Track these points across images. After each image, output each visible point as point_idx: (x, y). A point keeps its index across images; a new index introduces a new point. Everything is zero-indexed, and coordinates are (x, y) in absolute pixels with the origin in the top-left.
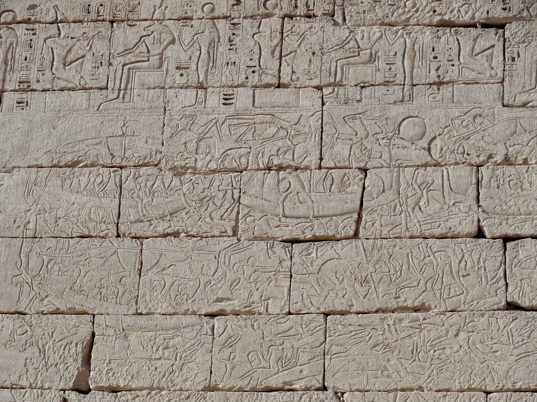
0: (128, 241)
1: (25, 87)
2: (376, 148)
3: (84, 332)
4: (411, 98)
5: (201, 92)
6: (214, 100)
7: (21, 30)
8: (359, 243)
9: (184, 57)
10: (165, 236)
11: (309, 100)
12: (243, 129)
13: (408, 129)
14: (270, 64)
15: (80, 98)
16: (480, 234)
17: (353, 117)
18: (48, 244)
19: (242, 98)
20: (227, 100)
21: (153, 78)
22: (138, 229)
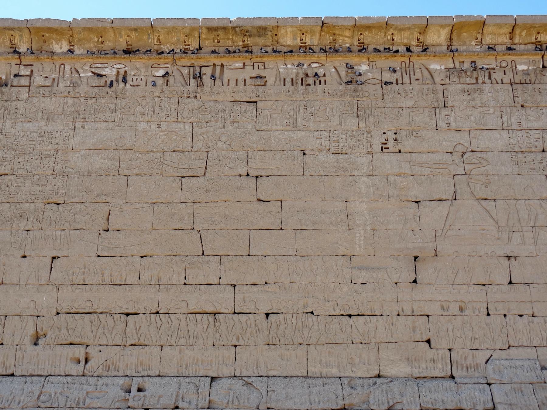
0: (122, 177)
1: (85, 120)
2: (212, 144)
3: (106, 208)
4: (224, 126)
5: (149, 124)
6: (154, 126)
7: (82, 100)
8: (206, 178)
9: (142, 110)
10: (136, 175)
11: (188, 127)
12: (164, 137)
13: (223, 138)
14: (174, 114)
15: (104, 125)
16: (248, 175)
17: (204, 133)
18: (93, 177)
19: (164, 126)
20: (159, 126)
21: (132, 118)
22: (127, 172)
